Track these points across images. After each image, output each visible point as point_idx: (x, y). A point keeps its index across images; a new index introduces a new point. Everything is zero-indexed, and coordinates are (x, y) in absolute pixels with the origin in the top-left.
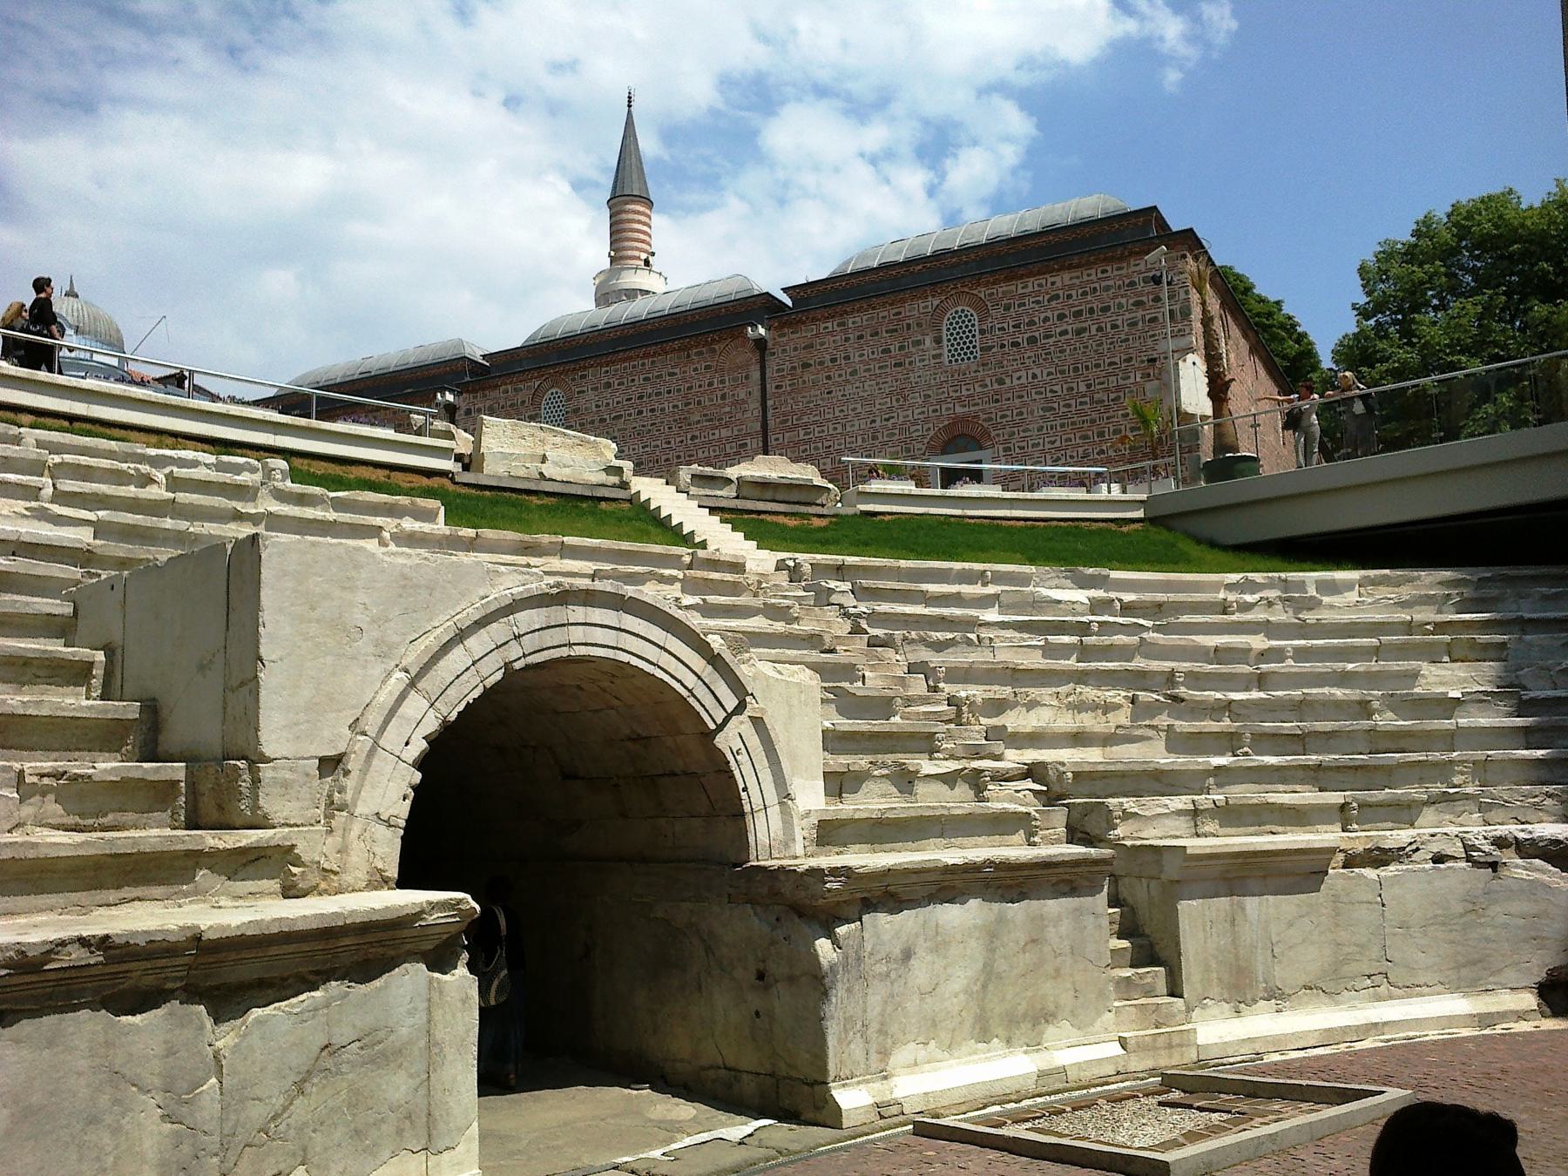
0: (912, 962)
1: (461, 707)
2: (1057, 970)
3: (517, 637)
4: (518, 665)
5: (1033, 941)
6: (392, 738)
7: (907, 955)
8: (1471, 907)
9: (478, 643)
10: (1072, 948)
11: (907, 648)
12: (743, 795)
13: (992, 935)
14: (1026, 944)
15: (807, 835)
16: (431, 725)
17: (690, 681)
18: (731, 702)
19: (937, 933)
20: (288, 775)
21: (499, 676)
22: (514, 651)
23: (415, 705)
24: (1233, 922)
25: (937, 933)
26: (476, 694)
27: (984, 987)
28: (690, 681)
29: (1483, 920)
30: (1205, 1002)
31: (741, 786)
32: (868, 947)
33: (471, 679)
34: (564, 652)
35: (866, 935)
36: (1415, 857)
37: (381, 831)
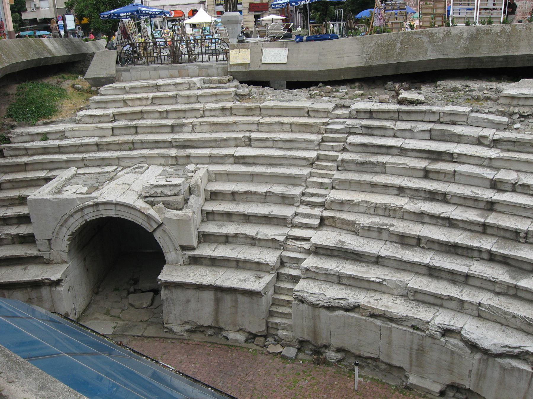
0: (190, 303)
1: (76, 229)
4: (88, 220)
6: (61, 236)
7: (188, 301)
11: (345, 165)
12: (162, 248)
20: (42, 243)
21: (84, 222)
23: (64, 230)
26: (79, 226)
31: (161, 246)
32: (175, 297)
34: (101, 216)
36: (405, 323)
37: (62, 253)
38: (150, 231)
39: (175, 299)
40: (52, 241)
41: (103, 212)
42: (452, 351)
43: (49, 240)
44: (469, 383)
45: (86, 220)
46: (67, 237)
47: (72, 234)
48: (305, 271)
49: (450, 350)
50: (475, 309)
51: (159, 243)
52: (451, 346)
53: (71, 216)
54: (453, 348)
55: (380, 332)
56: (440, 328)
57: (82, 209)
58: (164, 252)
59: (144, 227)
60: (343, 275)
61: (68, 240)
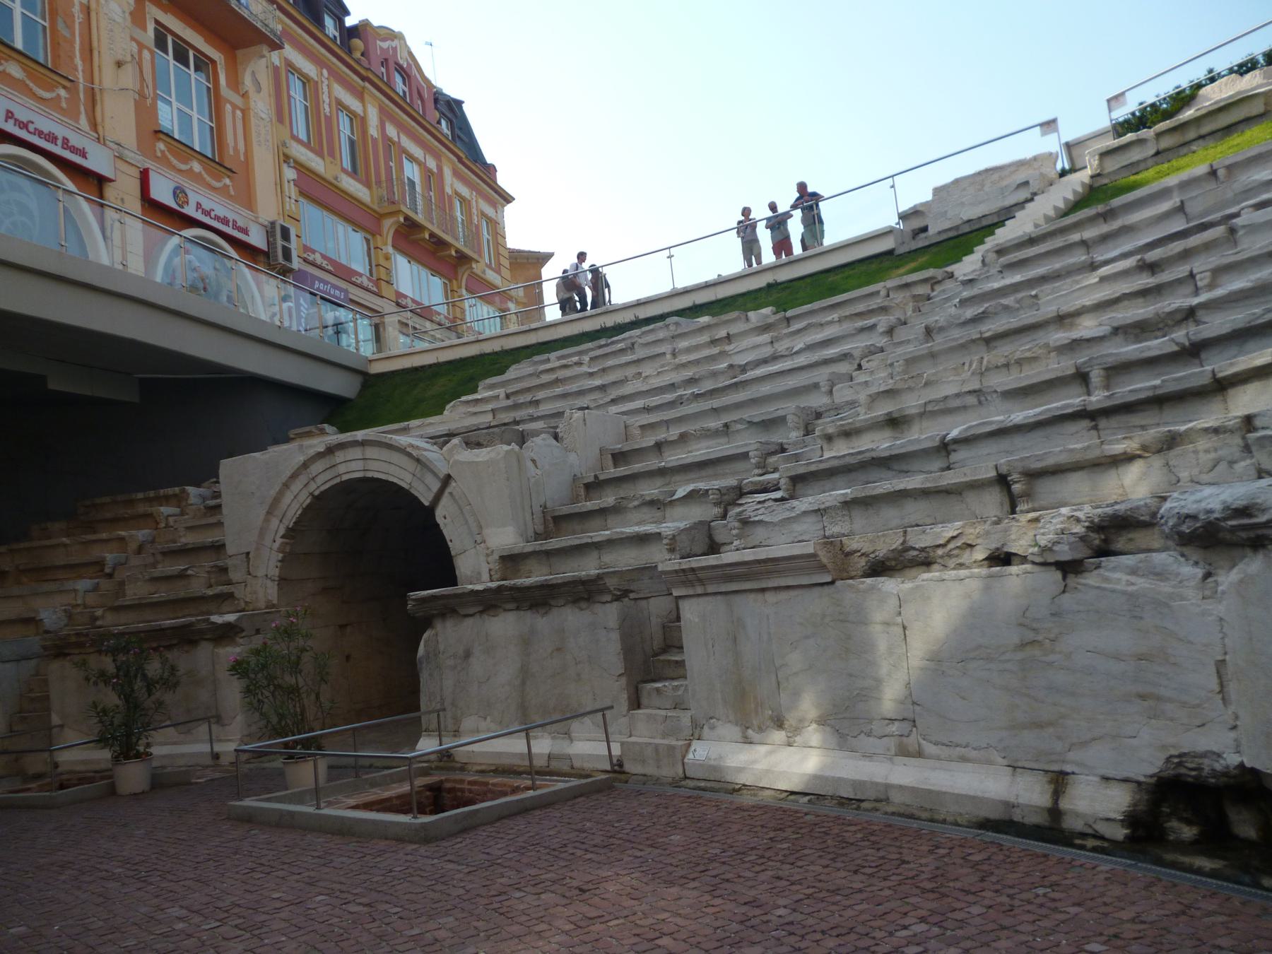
1: (294, 520)
2: (579, 675)
3: (313, 479)
4: (316, 493)
5: (558, 649)
7: (468, 655)
8: (1030, 636)
9: (297, 486)
10: (589, 657)
12: (449, 543)
13: (526, 642)
14: (553, 652)
15: (492, 567)
16: (282, 531)
17: (408, 478)
18: (436, 486)
19: (487, 640)
21: (308, 501)
22: (313, 487)
23: (275, 522)
24: (735, 640)
25: (487, 640)
27: (523, 683)
28: (408, 478)
29: (1051, 658)
30: (712, 721)
33: (296, 506)
34: (337, 480)
35: (440, 639)
37: (269, 583)
38: (426, 503)
39: (444, 652)
40: (251, 556)
41: (342, 469)
42: (1131, 596)
43: (248, 554)
44: (1233, 734)
45: (311, 494)
46: (279, 541)
47: (291, 533)
48: (737, 524)
49: (1124, 593)
50: (1237, 455)
51: (445, 532)
52: (1125, 577)
53: (286, 486)
54: (1133, 579)
55: (899, 620)
56: (1078, 520)
57: (305, 465)
58: (453, 553)
59: (416, 494)
60: (827, 504)
61: (279, 550)
